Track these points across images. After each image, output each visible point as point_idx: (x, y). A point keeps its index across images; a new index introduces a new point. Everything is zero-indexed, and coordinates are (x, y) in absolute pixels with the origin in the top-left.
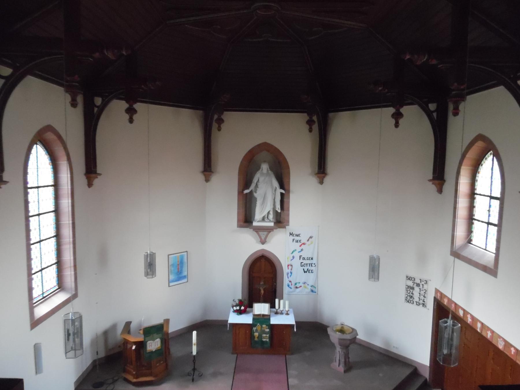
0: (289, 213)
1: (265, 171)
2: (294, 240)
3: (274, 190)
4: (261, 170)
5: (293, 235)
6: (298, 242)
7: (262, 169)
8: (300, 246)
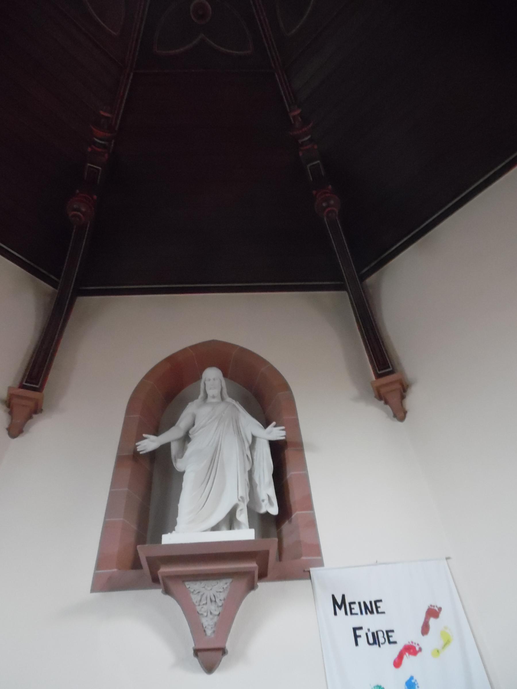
0: (313, 515)
1: (213, 391)
2: (358, 632)
3: (247, 446)
4: (202, 394)
5: (351, 609)
6: (382, 640)
7: (206, 396)
8: (398, 663)
